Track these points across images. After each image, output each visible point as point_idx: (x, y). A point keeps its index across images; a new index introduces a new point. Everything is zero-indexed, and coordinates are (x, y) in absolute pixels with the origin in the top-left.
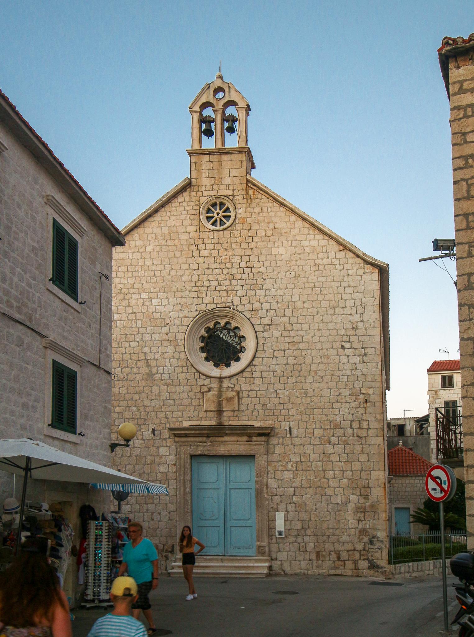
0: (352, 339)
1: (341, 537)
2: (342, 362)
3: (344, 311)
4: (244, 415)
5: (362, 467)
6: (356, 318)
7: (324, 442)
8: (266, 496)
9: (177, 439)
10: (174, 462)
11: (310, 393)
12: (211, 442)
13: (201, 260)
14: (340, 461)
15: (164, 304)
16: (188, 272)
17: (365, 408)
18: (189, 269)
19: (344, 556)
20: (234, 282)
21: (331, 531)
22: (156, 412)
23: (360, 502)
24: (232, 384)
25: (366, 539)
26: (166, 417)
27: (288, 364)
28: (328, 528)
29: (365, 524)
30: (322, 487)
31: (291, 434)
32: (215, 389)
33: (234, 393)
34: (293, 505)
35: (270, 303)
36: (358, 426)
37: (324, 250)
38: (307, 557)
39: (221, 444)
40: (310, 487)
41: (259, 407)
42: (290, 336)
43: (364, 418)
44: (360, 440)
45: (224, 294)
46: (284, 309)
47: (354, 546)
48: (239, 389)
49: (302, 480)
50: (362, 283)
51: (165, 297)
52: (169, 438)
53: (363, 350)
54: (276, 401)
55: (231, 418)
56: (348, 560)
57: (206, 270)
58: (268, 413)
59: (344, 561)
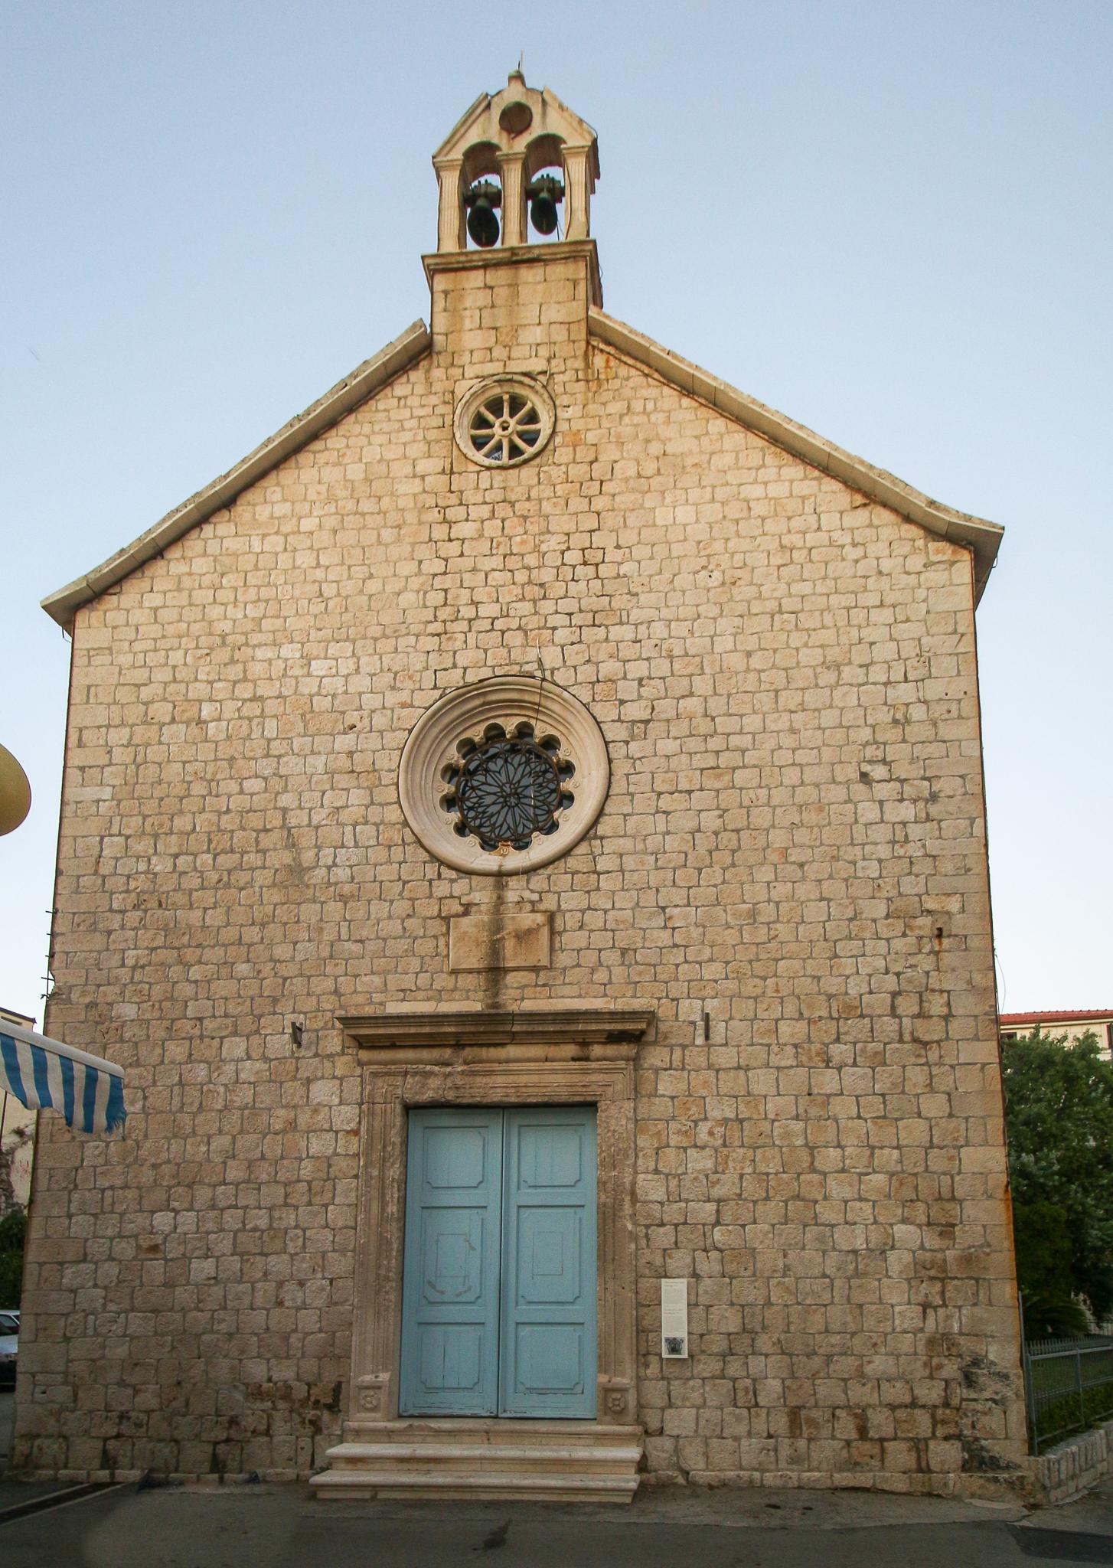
0: (891, 753)
1: (869, 1362)
2: (862, 820)
3: (867, 674)
4: (567, 981)
5: (931, 1136)
6: (904, 693)
7: (810, 1059)
8: (630, 1227)
9: (364, 1055)
10: (353, 1125)
11: (767, 912)
12: (466, 1063)
13: (454, 549)
14: (859, 1117)
15: (344, 671)
16: (415, 583)
17: (937, 953)
18: (419, 573)
19: (880, 1422)
20: (547, 607)
21: (835, 1339)
22: (309, 977)
23: (927, 1245)
24: (533, 891)
25: (951, 1369)
26: (336, 992)
27: (699, 830)
28: (827, 1331)
29: (948, 1317)
30: (803, 1200)
31: (707, 1037)
32: (483, 908)
33: (540, 918)
34: (714, 1254)
35: (648, 659)
36: (916, 1009)
37: (809, 509)
38: (761, 1426)
39: (496, 1067)
40: (767, 1199)
41: (611, 957)
42: (706, 752)
43: (933, 982)
44: (923, 1052)
45: (515, 639)
46: (691, 676)
47: (912, 1389)
48: (553, 907)
49: (742, 1176)
50: (921, 594)
51: (349, 653)
52: (343, 1053)
53: (926, 783)
54: (664, 938)
55: (528, 992)
56: (895, 1439)
57: (467, 576)
58: (640, 974)
59: (882, 1440)
